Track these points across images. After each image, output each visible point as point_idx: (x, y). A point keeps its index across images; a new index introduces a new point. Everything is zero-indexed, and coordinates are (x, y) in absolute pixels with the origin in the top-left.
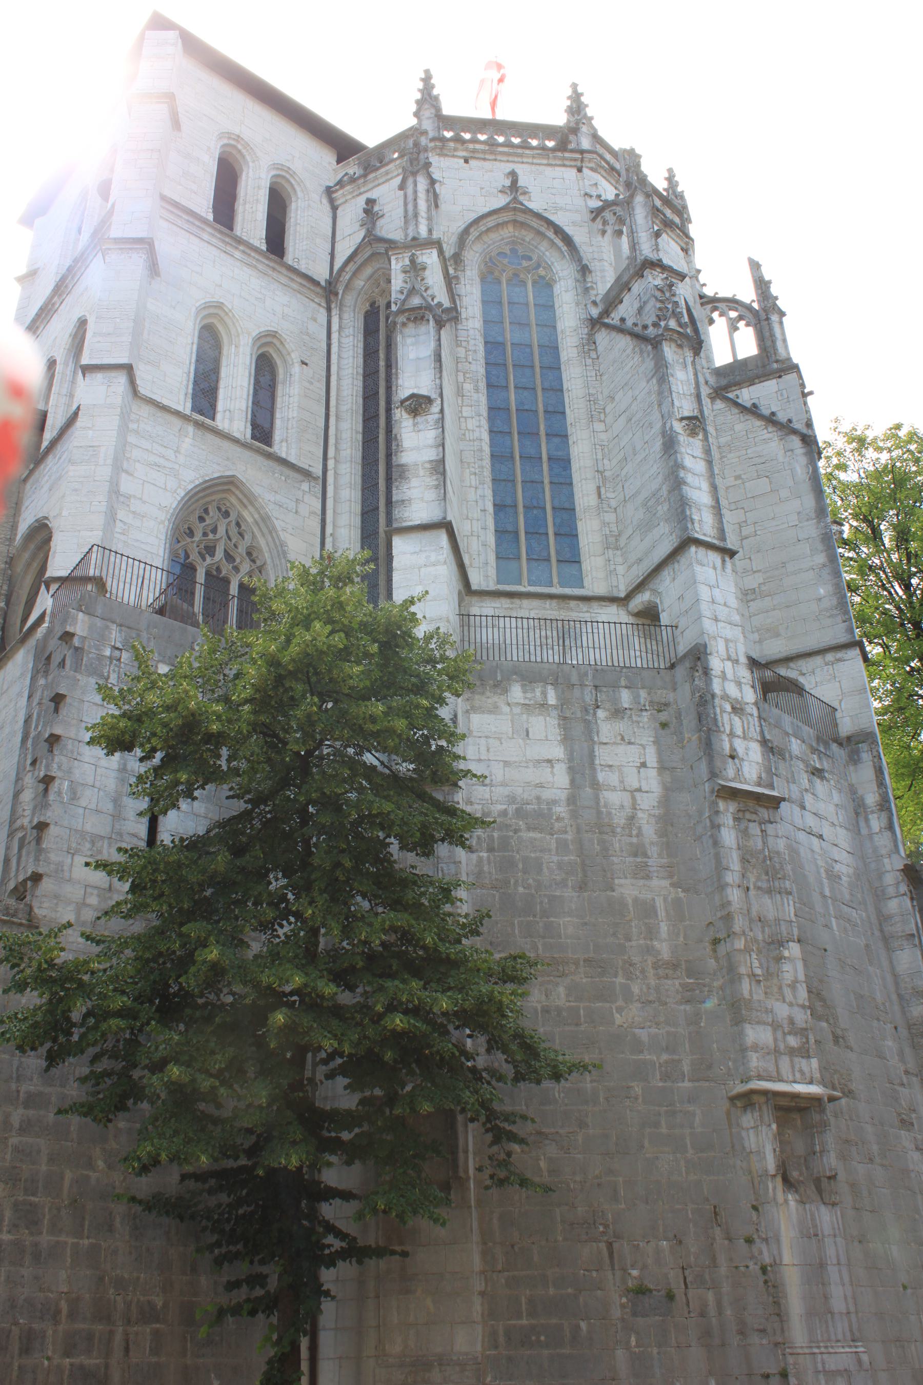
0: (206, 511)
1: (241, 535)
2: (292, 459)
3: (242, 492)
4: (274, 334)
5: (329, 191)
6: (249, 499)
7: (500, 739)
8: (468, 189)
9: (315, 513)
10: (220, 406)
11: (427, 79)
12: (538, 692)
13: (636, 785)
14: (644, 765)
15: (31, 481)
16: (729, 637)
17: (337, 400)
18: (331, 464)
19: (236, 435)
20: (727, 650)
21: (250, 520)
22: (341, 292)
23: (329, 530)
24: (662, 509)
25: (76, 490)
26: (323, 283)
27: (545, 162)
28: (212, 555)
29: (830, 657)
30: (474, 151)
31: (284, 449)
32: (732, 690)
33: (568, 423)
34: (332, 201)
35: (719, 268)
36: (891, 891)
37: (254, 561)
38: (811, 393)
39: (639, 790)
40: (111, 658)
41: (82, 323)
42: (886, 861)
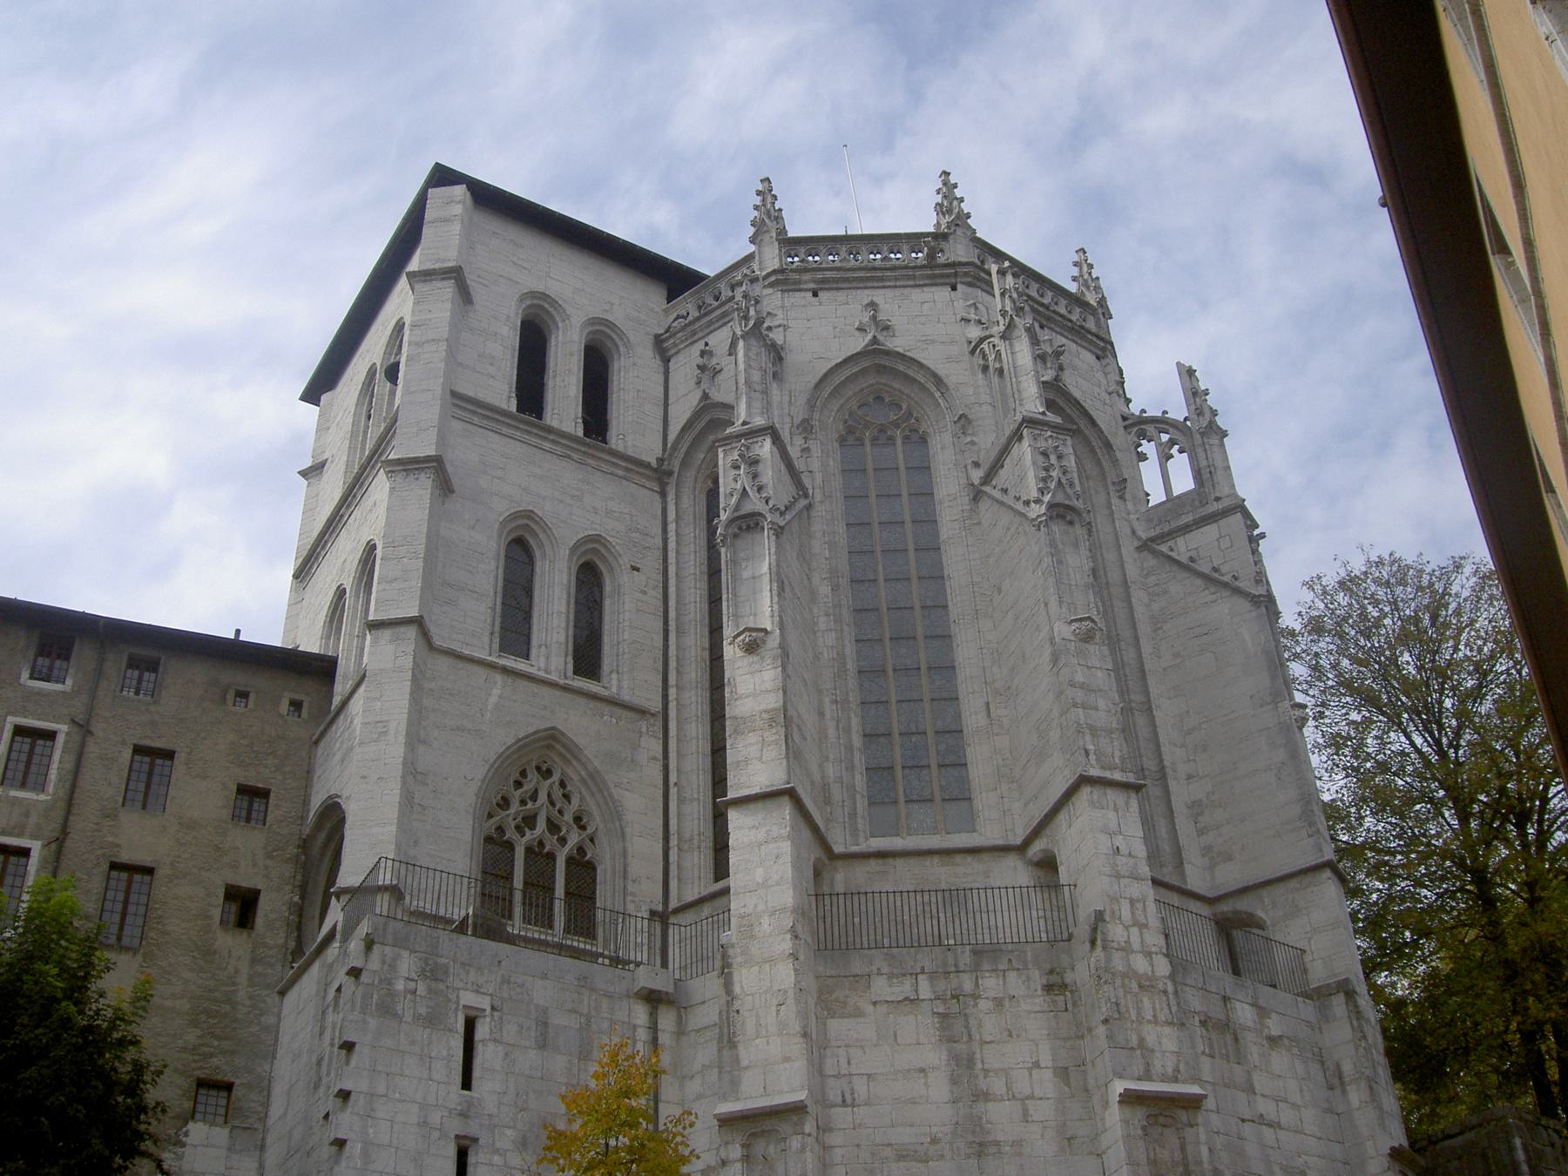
0: (523, 773)
1: (567, 797)
2: (626, 697)
3: (564, 746)
4: (597, 539)
5: (659, 341)
6: (572, 752)
7: (862, 1047)
8: (821, 332)
9: (654, 758)
10: (535, 641)
11: (766, 192)
13: (1027, 1091)
14: (1037, 1065)
15: (322, 744)
16: (1135, 896)
17: (677, 609)
18: (672, 692)
19: (554, 677)
20: (1133, 914)
21: (576, 778)
22: (676, 470)
23: (673, 778)
26: (654, 463)
28: (533, 828)
29: (1293, 883)
30: (824, 281)
31: (614, 682)
32: (1140, 964)
35: (1148, 374)
37: (583, 828)
38: (1262, 536)
39: (1031, 1097)
40: (407, 991)
41: (371, 548)
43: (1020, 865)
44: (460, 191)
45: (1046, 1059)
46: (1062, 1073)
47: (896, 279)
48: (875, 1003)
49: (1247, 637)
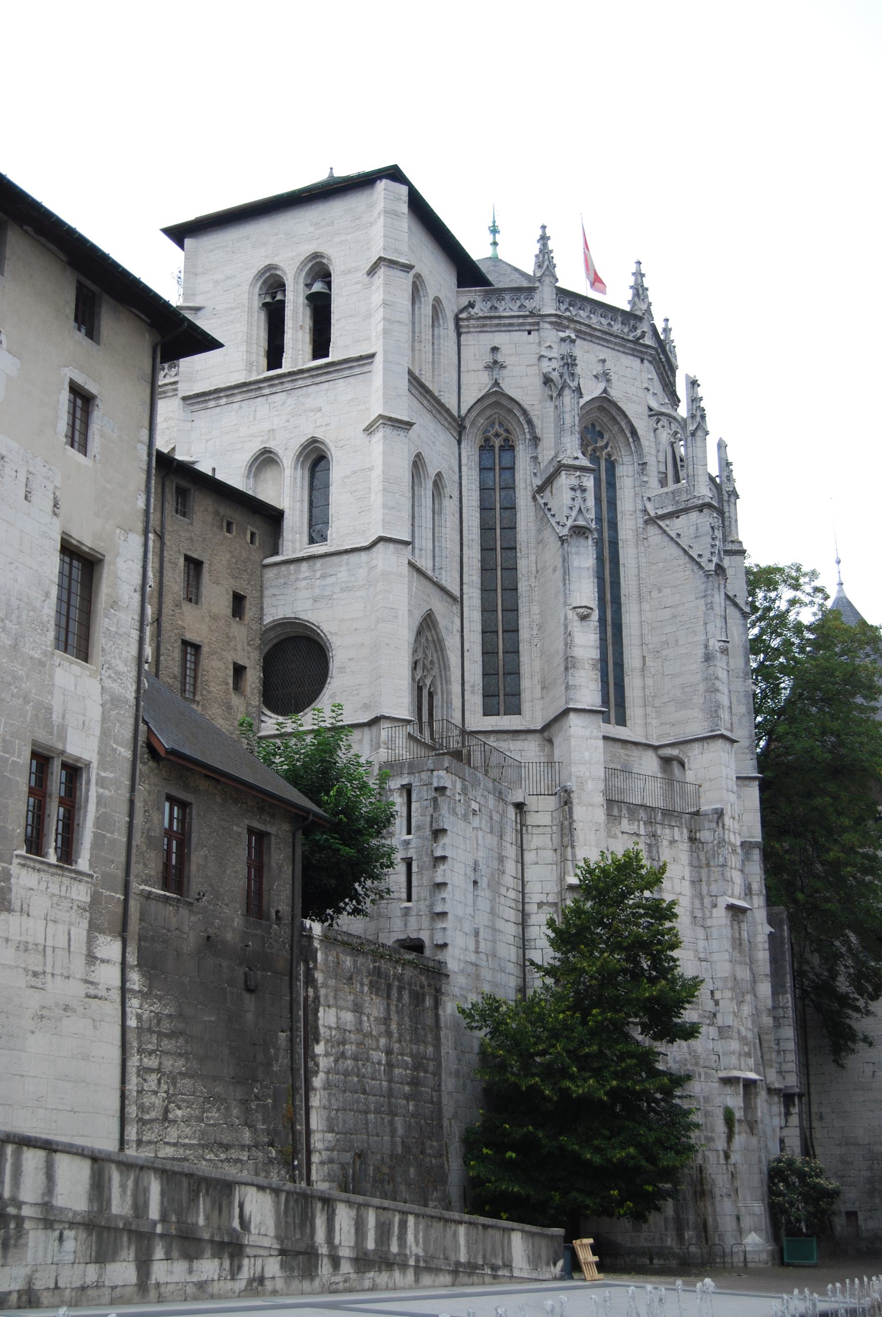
5: (457, 320)
12: (636, 827)
14: (683, 878)
24: (698, 700)
25: (387, 644)
27: (622, 349)
33: (622, 594)
34: (458, 327)
36: (760, 946)
39: (680, 894)
42: (759, 927)
43: (654, 755)
44: (404, 189)
45: (687, 877)
46: (693, 882)
47: (616, 344)
48: (623, 833)
49: (736, 634)
